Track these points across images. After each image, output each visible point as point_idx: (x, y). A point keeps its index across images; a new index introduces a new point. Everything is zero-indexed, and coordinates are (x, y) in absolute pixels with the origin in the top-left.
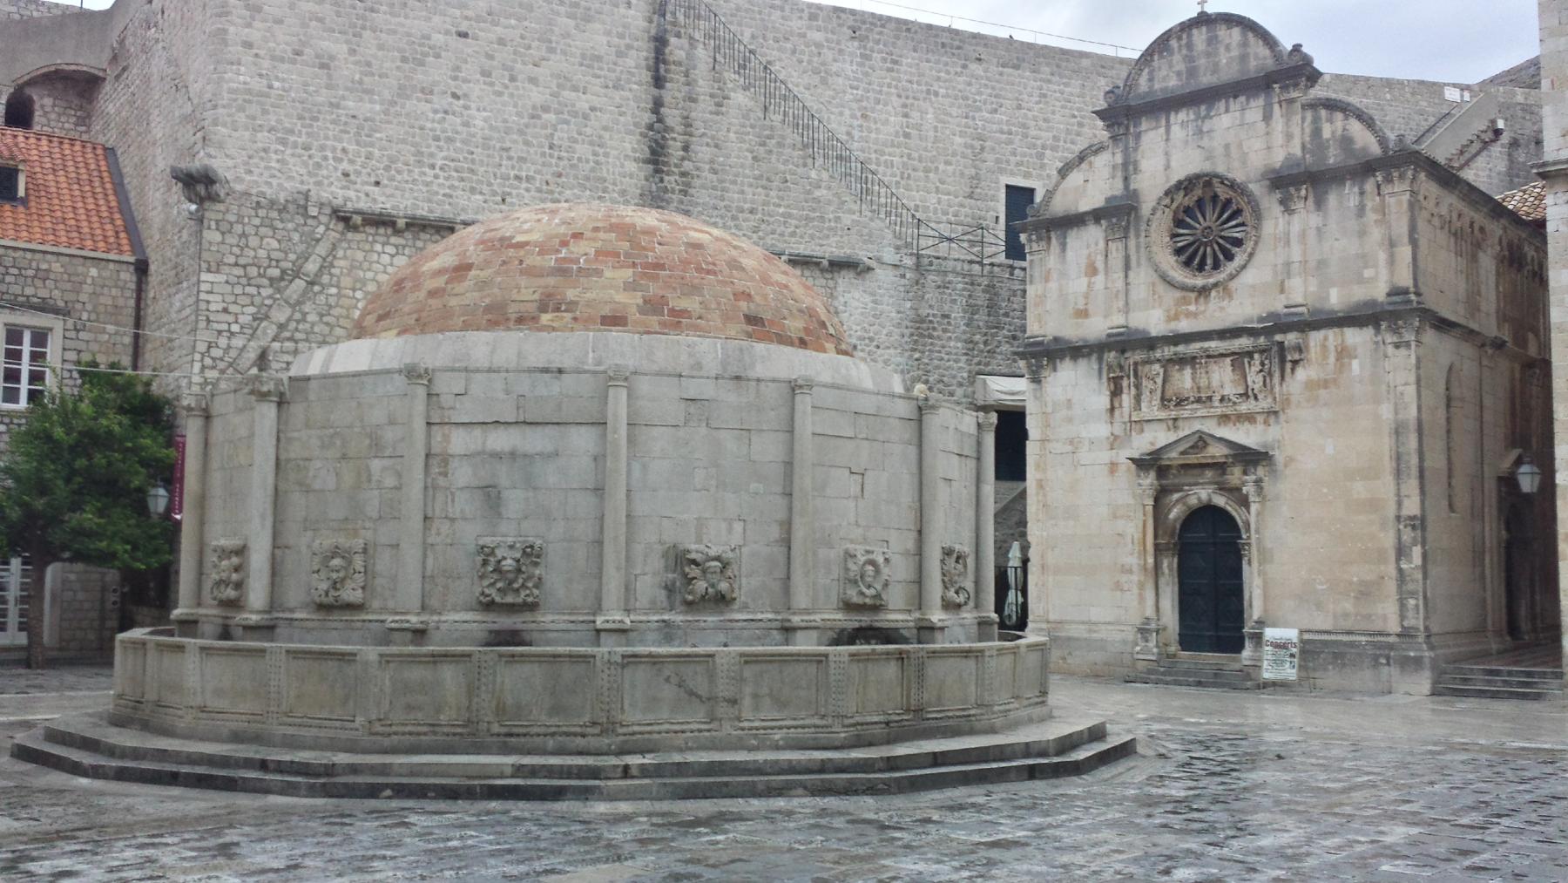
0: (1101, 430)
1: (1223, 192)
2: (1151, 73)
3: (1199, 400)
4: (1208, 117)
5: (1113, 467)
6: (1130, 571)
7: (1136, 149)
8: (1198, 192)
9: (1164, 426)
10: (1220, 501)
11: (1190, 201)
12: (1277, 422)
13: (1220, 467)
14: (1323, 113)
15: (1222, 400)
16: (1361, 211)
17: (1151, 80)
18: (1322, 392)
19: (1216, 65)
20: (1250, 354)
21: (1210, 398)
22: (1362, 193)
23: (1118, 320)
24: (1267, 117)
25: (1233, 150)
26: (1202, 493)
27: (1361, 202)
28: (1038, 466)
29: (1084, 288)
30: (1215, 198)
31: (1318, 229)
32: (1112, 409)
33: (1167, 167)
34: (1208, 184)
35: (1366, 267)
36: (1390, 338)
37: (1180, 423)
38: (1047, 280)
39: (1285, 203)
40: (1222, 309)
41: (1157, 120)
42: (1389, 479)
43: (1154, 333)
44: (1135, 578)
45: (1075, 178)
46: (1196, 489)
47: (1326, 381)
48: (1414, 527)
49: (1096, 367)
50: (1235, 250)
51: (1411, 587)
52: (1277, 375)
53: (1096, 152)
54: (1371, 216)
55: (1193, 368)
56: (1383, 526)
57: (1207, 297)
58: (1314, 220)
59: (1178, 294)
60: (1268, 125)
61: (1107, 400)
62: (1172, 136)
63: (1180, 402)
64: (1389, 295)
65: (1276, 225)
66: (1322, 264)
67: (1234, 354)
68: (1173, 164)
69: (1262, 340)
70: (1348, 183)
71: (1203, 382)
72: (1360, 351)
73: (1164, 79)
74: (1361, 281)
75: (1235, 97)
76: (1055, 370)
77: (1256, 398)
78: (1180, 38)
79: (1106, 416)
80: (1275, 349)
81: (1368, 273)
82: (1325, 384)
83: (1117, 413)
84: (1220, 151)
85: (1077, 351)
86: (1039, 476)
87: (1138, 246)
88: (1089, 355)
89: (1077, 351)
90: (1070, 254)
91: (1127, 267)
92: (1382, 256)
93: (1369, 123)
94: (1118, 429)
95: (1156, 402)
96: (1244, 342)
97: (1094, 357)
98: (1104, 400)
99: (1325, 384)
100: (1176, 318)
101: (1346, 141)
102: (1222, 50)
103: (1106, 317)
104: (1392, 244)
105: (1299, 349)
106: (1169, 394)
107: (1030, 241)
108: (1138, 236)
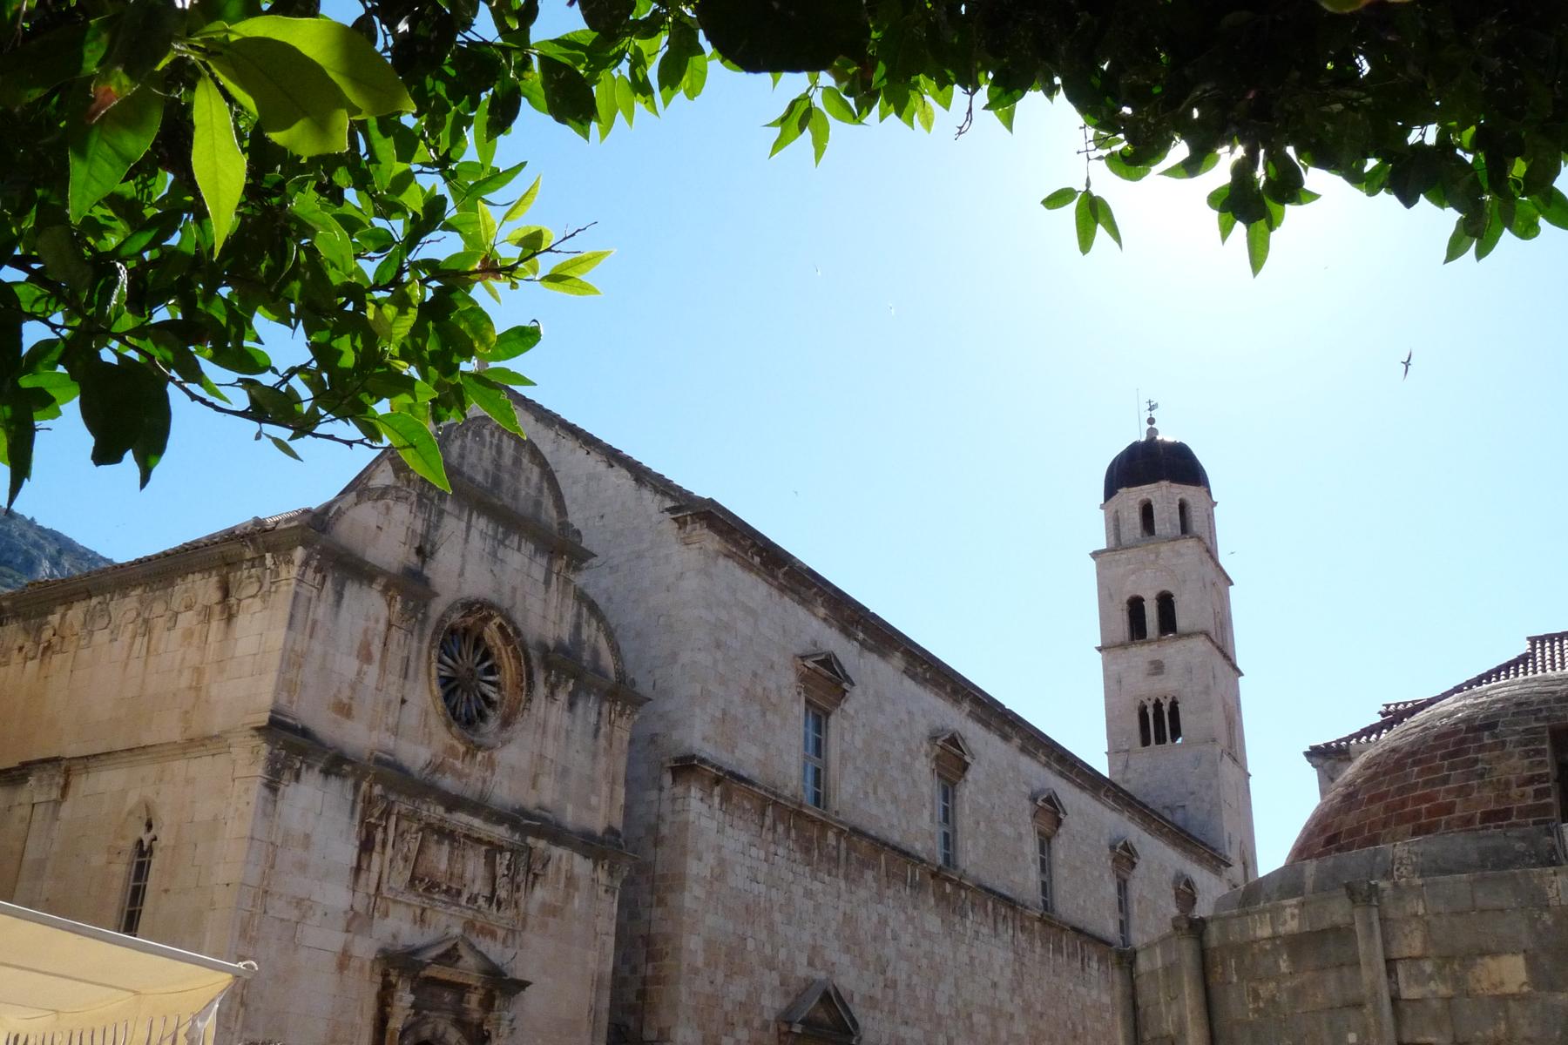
0: (337, 896)
1: (491, 633)
2: (463, 448)
3: (448, 891)
4: (502, 542)
7: (437, 527)
8: (470, 620)
16: (597, 730)
18: (551, 920)
20: (501, 849)
21: (459, 893)
22: (600, 714)
24: (547, 582)
30: (479, 640)
31: (567, 732)
32: (358, 870)
33: (461, 574)
34: (489, 618)
41: (461, 511)
49: (350, 797)
50: (489, 712)
55: (451, 845)
58: (566, 718)
61: (356, 851)
67: (490, 843)
68: (467, 574)
71: (458, 868)
73: (473, 466)
74: (589, 808)
76: (297, 777)
78: (492, 435)
79: (347, 877)
81: (594, 800)
83: (363, 876)
84: (507, 590)
85: (336, 763)
87: (419, 651)
88: (343, 776)
89: (336, 763)
91: (406, 677)
92: (605, 790)
93: (615, 649)
96: (501, 833)
97: (350, 782)
98: (348, 853)
101: (596, 653)
102: (523, 479)
103: (372, 728)
104: (614, 782)
106: (421, 870)
107: (305, 563)
108: (421, 641)
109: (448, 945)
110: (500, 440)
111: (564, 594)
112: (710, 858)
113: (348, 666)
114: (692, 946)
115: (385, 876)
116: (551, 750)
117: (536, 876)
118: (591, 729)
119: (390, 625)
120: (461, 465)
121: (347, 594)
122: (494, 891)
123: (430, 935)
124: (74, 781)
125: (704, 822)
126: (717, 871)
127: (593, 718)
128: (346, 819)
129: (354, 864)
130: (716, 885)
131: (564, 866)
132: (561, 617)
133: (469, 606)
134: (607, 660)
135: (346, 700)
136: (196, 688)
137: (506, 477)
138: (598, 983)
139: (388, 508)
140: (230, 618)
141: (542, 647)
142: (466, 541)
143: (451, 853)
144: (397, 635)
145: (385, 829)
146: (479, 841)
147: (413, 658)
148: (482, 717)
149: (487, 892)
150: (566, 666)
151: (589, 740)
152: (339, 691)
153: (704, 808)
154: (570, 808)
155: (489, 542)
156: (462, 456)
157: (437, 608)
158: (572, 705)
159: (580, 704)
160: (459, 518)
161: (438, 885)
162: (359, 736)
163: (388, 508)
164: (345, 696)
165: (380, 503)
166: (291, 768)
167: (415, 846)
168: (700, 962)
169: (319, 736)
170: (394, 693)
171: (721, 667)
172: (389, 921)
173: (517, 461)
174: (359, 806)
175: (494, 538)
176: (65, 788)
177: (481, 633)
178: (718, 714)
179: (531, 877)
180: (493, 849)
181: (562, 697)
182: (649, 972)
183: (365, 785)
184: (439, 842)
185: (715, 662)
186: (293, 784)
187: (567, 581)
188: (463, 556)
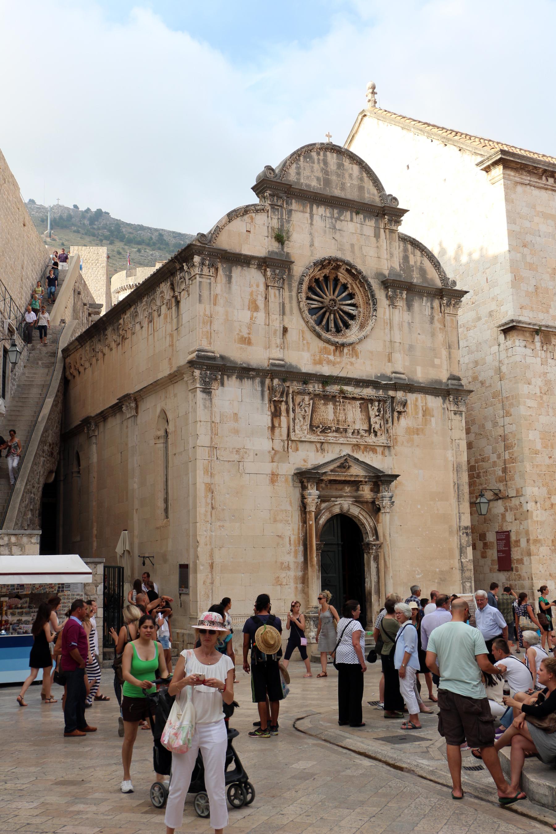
0: (263, 444)
2: (298, 168)
3: (337, 430)
4: (338, 219)
5: (274, 477)
6: (288, 568)
7: (288, 221)
8: (326, 271)
9: (313, 447)
10: (355, 511)
11: (320, 275)
12: (390, 455)
13: (356, 484)
14: (409, 247)
15: (353, 433)
16: (432, 318)
17: (298, 174)
18: (415, 436)
19: (343, 184)
20: (371, 401)
21: (346, 430)
22: (432, 308)
23: (276, 353)
24: (377, 236)
25: (356, 248)
26: (345, 504)
27: (432, 313)
28: (206, 471)
29: (248, 320)
30: (336, 280)
31: (409, 324)
32: (273, 428)
33: (312, 245)
34: (337, 268)
35: (436, 357)
36: (453, 408)
37: (325, 446)
38: (215, 304)
39: (391, 300)
40: (352, 364)
42: (453, 501)
43: (304, 370)
44: (292, 573)
45: (239, 225)
46: (339, 501)
47: (417, 429)
48: (467, 534)
49: (259, 389)
50: (351, 322)
51: (467, 574)
52: (390, 420)
53: (257, 211)
54: (437, 325)
55: (334, 405)
56: (451, 532)
57: (341, 352)
58: (407, 316)
59: (321, 344)
60: (377, 241)
61: (269, 418)
62: (314, 222)
63: (325, 430)
64: (448, 379)
65: (385, 312)
66: (411, 348)
67: (362, 399)
68: (316, 244)
69: (381, 392)
70: (425, 299)
71: (342, 417)
72: (435, 413)
73: (308, 177)
74: (433, 366)
75: (357, 213)
76: (222, 384)
77: (376, 435)
78: (318, 154)
79: (268, 433)
80: (389, 401)
81: (437, 361)
82: (417, 431)
83: (277, 431)
84: (347, 247)
85: (245, 372)
86: (208, 480)
87: (291, 297)
88: (253, 378)
89: (245, 372)
90: (234, 286)
91: (284, 314)
92: (444, 353)
94: (278, 445)
95: (306, 427)
96: (368, 392)
97: (258, 380)
98: (266, 419)
99: (417, 431)
100: (320, 362)
101: (423, 272)
102: (347, 176)
105: (405, 404)
107: (202, 264)
108: (290, 290)
109: (342, 460)
110: (325, 155)
111: (391, 240)
112: (539, 382)
113: (245, 315)
114: (531, 437)
115: (291, 428)
116: (397, 338)
117: (400, 413)
118: (428, 319)
119: (267, 286)
120: (299, 179)
121: (233, 275)
122: (370, 426)
123: (329, 457)
124: (140, 404)
125: (529, 360)
126: (546, 388)
127: (428, 312)
128: (259, 401)
129: (270, 425)
130: (545, 397)
131: (420, 404)
132: (392, 255)
133: (322, 264)
134: (432, 273)
135: (246, 336)
136: (172, 345)
137: (334, 178)
138: (458, 469)
139: (252, 218)
140: (178, 303)
141: (379, 275)
142: (311, 224)
143: (335, 409)
144: (271, 291)
145: (287, 403)
146: (354, 399)
147: (287, 301)
148: (347, 326)
149: (366, 427)
150: (400, 287)
151: (427, 326)
152: (240, 330)
153: (528, 351)
154: (419, 369)
155: (328, 221)
156: (298, 174)
157: (298, 269)
158: (409, 306)
159: (416, 305)
160: (303, 212)
161: (330, 428)
162: (258, 356)
163: (252, 218)
164: (245, 333)
165: (246, 217)
166: (216, 379)
167: (309, 410)
168: (539, 447)
169: (232, 359)
170: (277, 325)
171: (528, 259)
172: (299, 453)
173: (340, 166)
174: (267, 393)
175: (332, 217)
176: (137, 408)
177: (337, 276)
178: (531, 289)
179: (396, 414)
180: (366, 402)
181: (401, 303)
182: (507, 457)
183: (268, 381)
184: (325, 404)
185: (524, 256)
186: (220, 388)
187: (392, 231)
188: (311, 234)
